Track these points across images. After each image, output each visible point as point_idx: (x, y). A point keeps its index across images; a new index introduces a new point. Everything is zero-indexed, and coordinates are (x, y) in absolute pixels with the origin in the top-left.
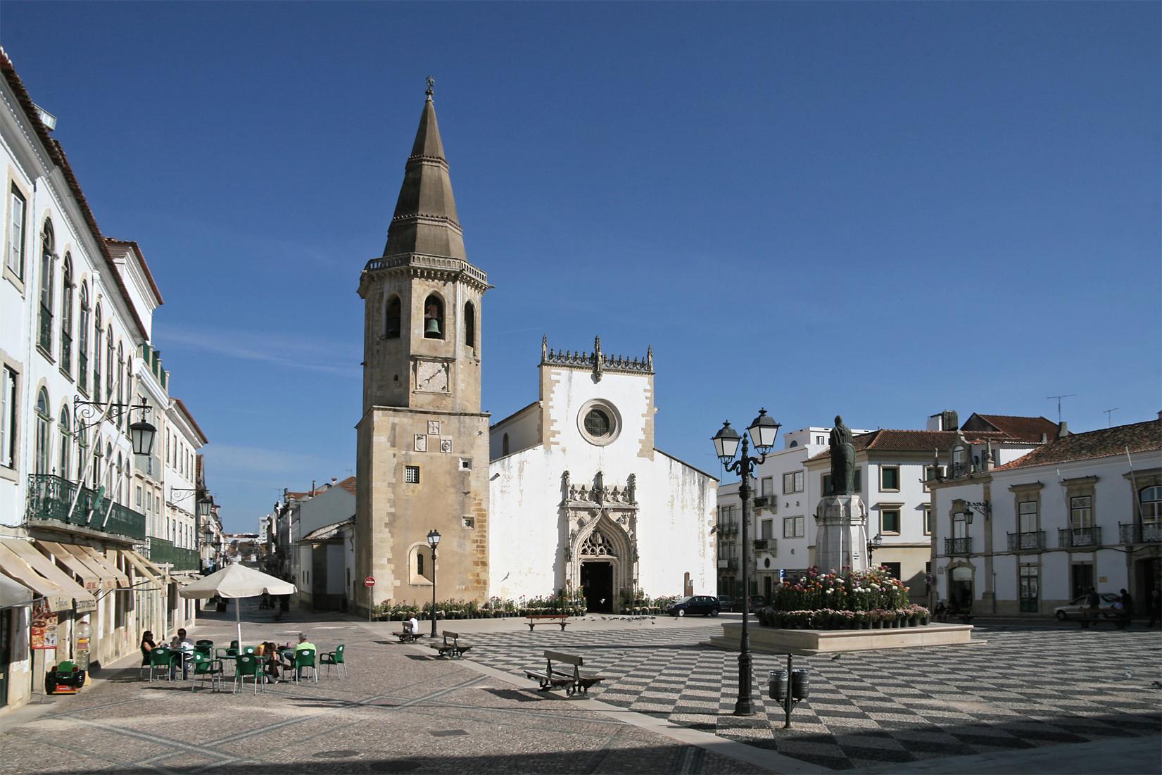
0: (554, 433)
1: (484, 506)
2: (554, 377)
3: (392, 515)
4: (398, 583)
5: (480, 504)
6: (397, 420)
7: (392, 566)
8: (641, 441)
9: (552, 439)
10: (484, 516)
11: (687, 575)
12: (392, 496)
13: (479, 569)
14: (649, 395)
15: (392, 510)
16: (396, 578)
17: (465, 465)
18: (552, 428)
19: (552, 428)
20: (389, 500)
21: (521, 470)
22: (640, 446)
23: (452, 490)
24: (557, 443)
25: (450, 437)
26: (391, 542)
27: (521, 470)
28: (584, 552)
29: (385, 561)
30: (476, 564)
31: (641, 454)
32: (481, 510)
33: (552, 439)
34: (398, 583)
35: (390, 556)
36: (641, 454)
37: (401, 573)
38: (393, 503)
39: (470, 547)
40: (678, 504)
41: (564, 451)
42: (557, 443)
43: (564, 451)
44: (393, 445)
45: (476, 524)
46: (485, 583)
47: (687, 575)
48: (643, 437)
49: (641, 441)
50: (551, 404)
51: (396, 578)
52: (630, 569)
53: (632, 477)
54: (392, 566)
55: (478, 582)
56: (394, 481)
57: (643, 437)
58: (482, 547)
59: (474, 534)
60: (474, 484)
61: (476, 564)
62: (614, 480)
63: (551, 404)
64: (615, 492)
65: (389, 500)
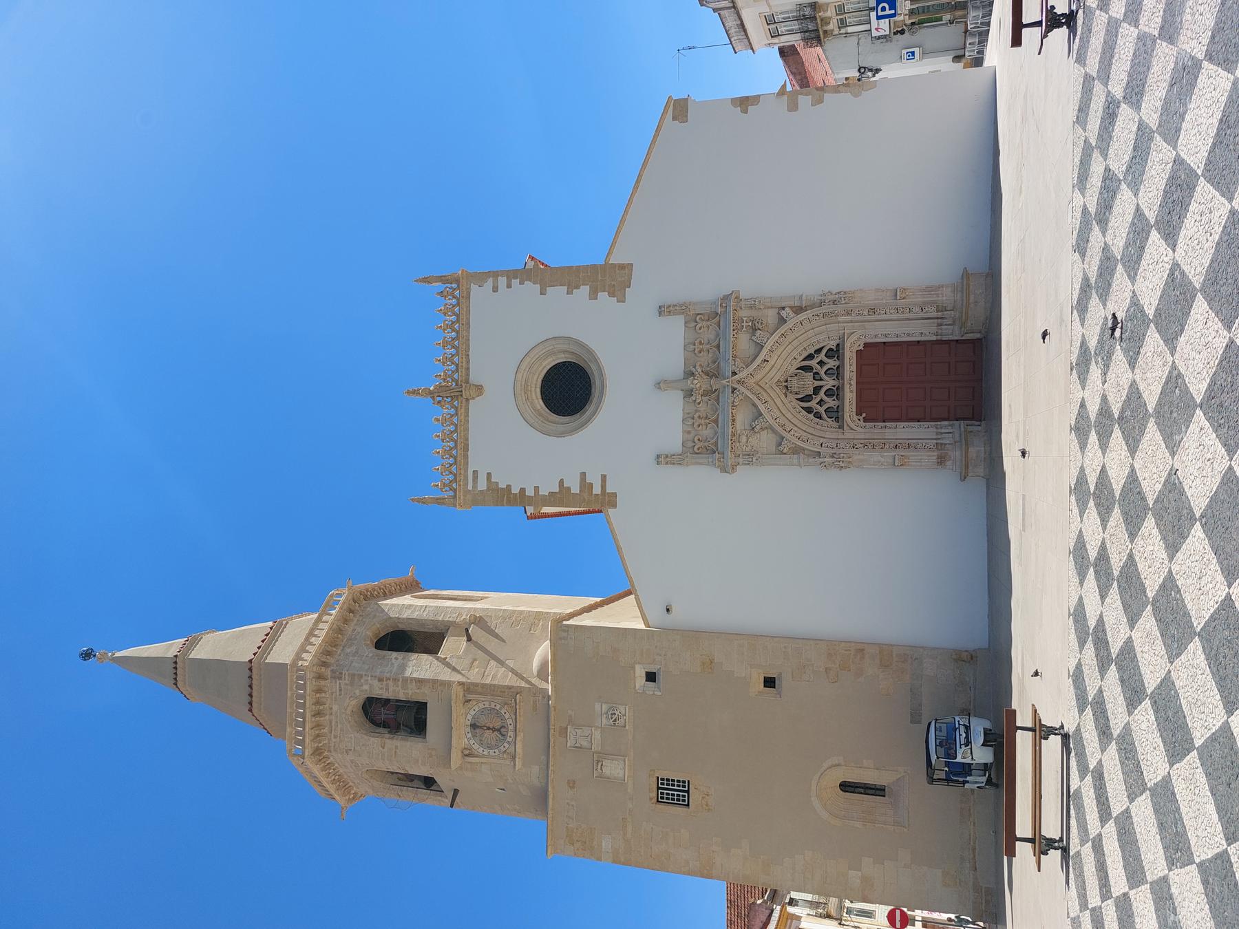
0: (585, 486)
2: (482, 485)
8: (593, 295)
9: (597, 490)
14: (502, 281)
17: (651, 677)
18: (575, 489)
19: (575, 489)
22: (603, 296)
24: (604, 478)
25: (597, 706)
28: (835, 414)
33: (597, 490)
42: (604, 478)
48: (585, 290)
49: (593, 295)
57: (585, 290)
63: (530, 492)
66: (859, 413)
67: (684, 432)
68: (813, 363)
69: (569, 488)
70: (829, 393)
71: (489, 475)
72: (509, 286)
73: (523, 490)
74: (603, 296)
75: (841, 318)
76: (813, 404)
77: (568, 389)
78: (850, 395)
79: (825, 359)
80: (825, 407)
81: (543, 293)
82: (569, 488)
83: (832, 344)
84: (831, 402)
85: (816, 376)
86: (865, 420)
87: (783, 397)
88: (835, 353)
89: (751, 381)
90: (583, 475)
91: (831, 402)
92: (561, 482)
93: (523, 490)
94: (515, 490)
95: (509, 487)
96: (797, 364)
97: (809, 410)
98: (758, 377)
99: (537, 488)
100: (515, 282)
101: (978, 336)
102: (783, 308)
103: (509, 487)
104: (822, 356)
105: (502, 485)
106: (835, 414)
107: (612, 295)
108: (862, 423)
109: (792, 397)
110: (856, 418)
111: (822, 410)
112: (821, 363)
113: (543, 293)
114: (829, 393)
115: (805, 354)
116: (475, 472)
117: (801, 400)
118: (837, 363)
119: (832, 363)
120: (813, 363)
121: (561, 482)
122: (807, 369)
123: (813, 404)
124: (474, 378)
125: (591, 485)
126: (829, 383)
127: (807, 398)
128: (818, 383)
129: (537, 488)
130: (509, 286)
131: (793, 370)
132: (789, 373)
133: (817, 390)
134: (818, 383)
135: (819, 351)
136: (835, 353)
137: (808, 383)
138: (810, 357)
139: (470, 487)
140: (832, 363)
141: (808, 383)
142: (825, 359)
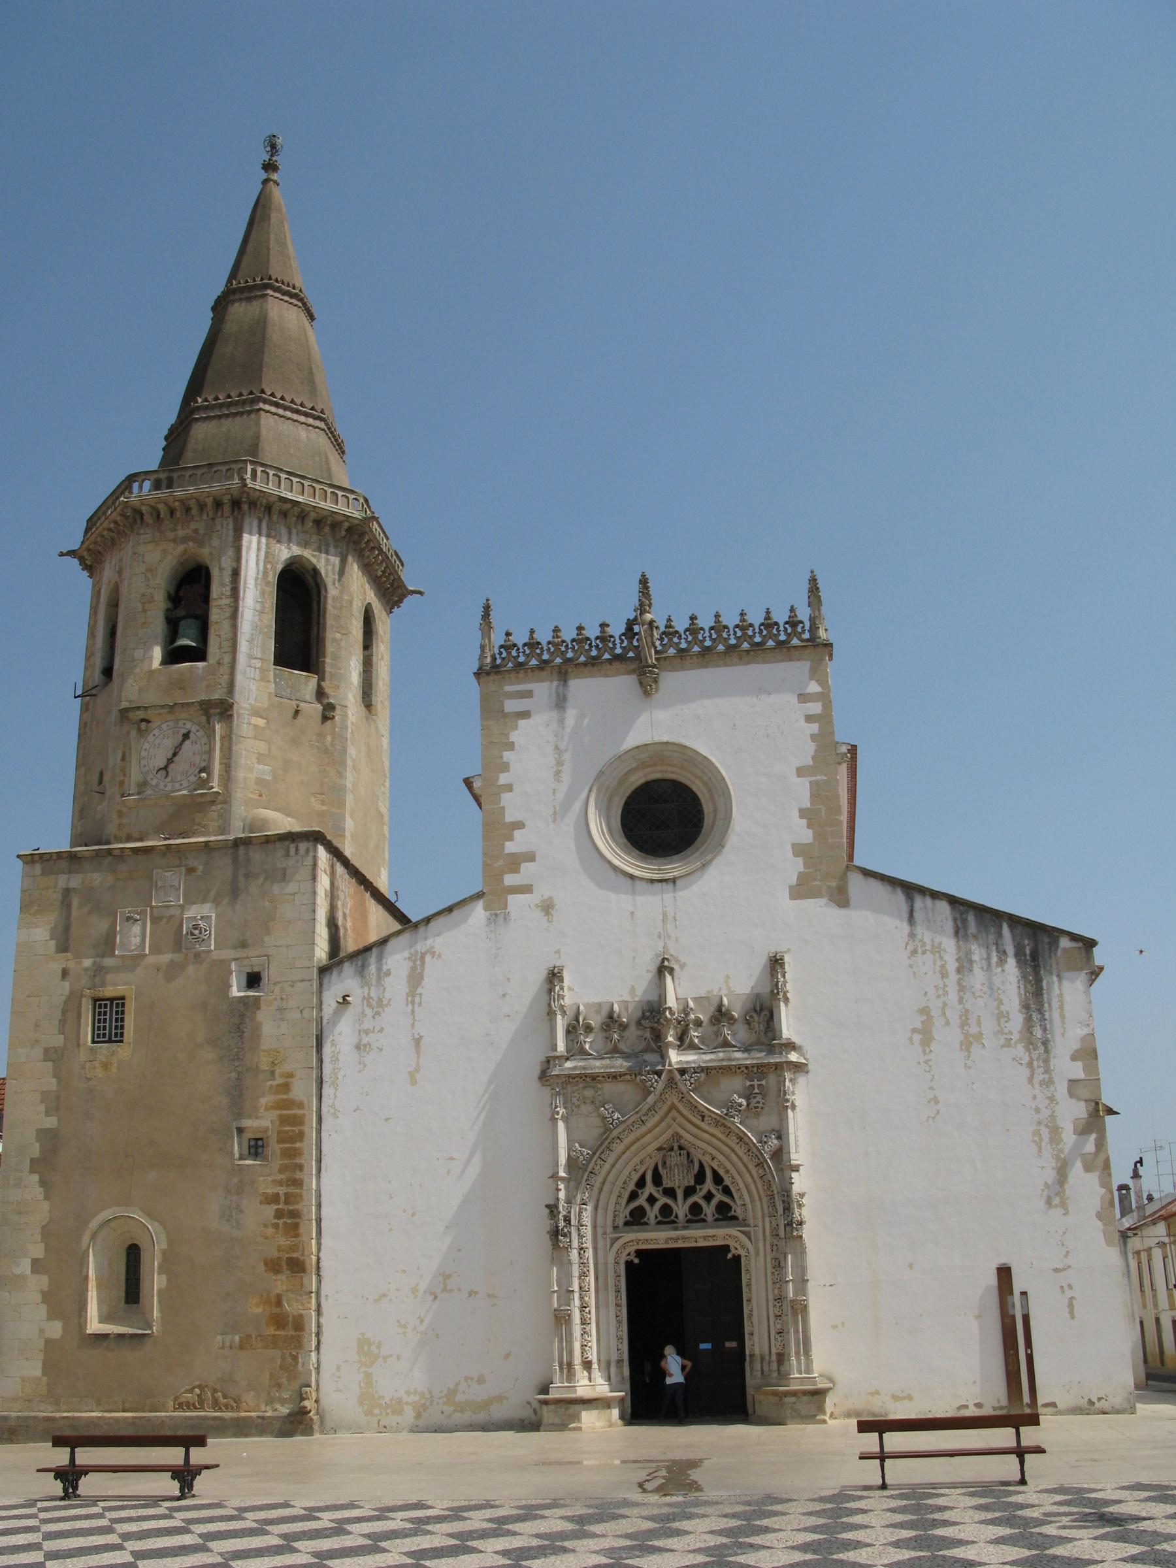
0: (515, 862)
1: (301, 1089)
2: (511, 706)
3: (49, 1138)
4: (55, 1329)
5: (286, 1087)
6: (75, 881)
7: (43, 1281)
8: (799, 850)
9: (510, 880)
10: (298, 1121)
11: (1004, 1273)
12: (52, 1084)
13: (280, 1283)
14: (815, 708)
15: (51, 1122)
16: (51, 1316)
17: (253, 980)
18: (510, 847)
19: (510, 847)
20: (45, 1096)
21: (415, 979)
22: (797, 866)
23: (208, 1054)
26: (42, 1211)
27: (415, 979)
29: (24, 1267)
30: (273, 1266)
31: (802, 890)
32: (289, 1104)
33: (510, 880)
34: (55, 1329)
35: (37, 1250)
36: (802, 890)
37: (65, 1302)
38: (54, 1103)
39: (257, 1216)
40: (947, 1036)
41: (547, 907)
42: (526, 889)
43: (547, 907)
44: (63, 947)
45: (274, 1148)
46: (299, 1324)
47: (1004, 1273)
48: (806, 835)
49: (799, 850)
50: (503, 779)
51: (51, 1316)
52: (779, 1265)
53: (776, 963)
54: (43, 1281)
55: (279, 1321)
56: (58, 1041)
57: (806, 835)
58: (291, 1213)
59: (266, 1176)
60: (272, 1029)
61: (273, 1266)
62: (714, 975)
63: (503, 779)
64: (721, 1015)
65: (45, 1094)
66: (639, 1253)
67: (600, 1005)
68: (709, 1185)
69: (511, 839)
70: (666, 1210)
71: (526, 715)
72: (809, 719)
73: (505, 767)
74: (799, 865)
75: (767, 1220)
76: (650, 1188)
77: (665, 817)
78: (658, 1238)
79: (714, 1202)
80: (646, 1206)
81: (800, 772)
82: (511, 839)
83: (737, 1210)
84: (652, 1213)
85: (689, 1191)
86: (629, 1264)
87: (656, 1144)
88: (725, 1213)
89: (673, 1098)
90: (531, 857)
91: (652, 1213)
92: (520, 825)
93: (505, 767)
94: (508, 756)
95: (511, 746)
96: (706, 1160)
97: (641, 1183)
98: (680, 1107)
99: (509, 788)
100: (815, 728)
101: (750, 1411)
102: (779, 1138)
103: (511, 746)
104: (719, 1197)
105: (514, 736)
106: (637, 1218)
107: (801, 876)
108: (623, 1259)
109: (658, 1158)
110: (632, 1249)
111: (642, 1201)
112: (709, 1197)
113: (800, 772)
114: (666, 1210)
115: (721, 1172)
116: (528, 694)
117: (656, 1169)
118: (710, 1218)
119: (709, 1210)
120: (709, 1185)
121: (520, 825)
122: (700, 1178)
123: (650, 1188)
124: (670, 680)
125: (516, 870)
126: (681, 1209)
127: (657, 1179)
128: (680, 1194)
129: (509, 788)
130: (809, 719)
131: (697, 1155)
132: (692, 1150)
133: (670, 1193)
134: (680, 1194)
135: (727, 1191)
136: (725, 1213)
137: (678, 1179)
138: (718, 1179)
139: (508, 688)
140: (709, 1210)
141: (678, 1179)
142: (714, 1202)
